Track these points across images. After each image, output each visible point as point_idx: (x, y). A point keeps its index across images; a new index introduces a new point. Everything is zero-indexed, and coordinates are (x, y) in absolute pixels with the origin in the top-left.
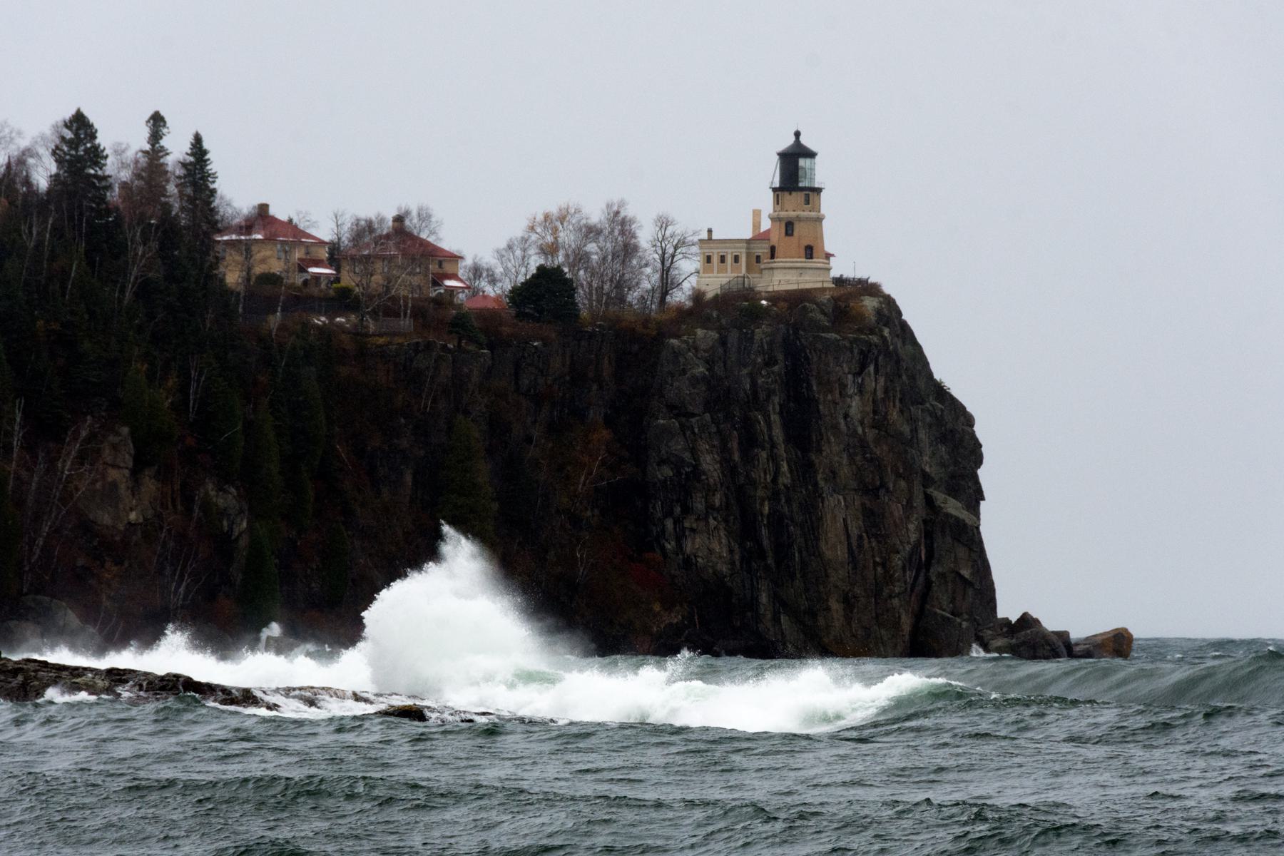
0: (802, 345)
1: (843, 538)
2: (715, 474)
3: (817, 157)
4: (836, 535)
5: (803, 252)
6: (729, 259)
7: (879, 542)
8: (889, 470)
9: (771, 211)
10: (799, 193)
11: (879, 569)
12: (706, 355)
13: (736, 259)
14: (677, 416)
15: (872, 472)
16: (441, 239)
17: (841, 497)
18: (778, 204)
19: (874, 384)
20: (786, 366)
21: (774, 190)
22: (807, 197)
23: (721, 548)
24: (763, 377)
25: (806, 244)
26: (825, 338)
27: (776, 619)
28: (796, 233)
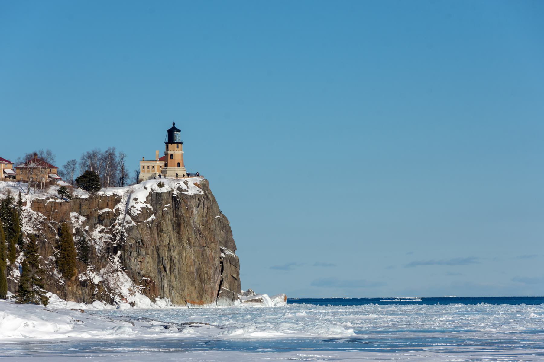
3: (181, 132)
5: (176, 165)
6: (151, 167)
7: (206, 265)
8: (208, 240)
11: (206, 275)
16: (55, 162)
17: (192, 250)
19: (203, 210)
21: (166, 143)
25: (178, 162)
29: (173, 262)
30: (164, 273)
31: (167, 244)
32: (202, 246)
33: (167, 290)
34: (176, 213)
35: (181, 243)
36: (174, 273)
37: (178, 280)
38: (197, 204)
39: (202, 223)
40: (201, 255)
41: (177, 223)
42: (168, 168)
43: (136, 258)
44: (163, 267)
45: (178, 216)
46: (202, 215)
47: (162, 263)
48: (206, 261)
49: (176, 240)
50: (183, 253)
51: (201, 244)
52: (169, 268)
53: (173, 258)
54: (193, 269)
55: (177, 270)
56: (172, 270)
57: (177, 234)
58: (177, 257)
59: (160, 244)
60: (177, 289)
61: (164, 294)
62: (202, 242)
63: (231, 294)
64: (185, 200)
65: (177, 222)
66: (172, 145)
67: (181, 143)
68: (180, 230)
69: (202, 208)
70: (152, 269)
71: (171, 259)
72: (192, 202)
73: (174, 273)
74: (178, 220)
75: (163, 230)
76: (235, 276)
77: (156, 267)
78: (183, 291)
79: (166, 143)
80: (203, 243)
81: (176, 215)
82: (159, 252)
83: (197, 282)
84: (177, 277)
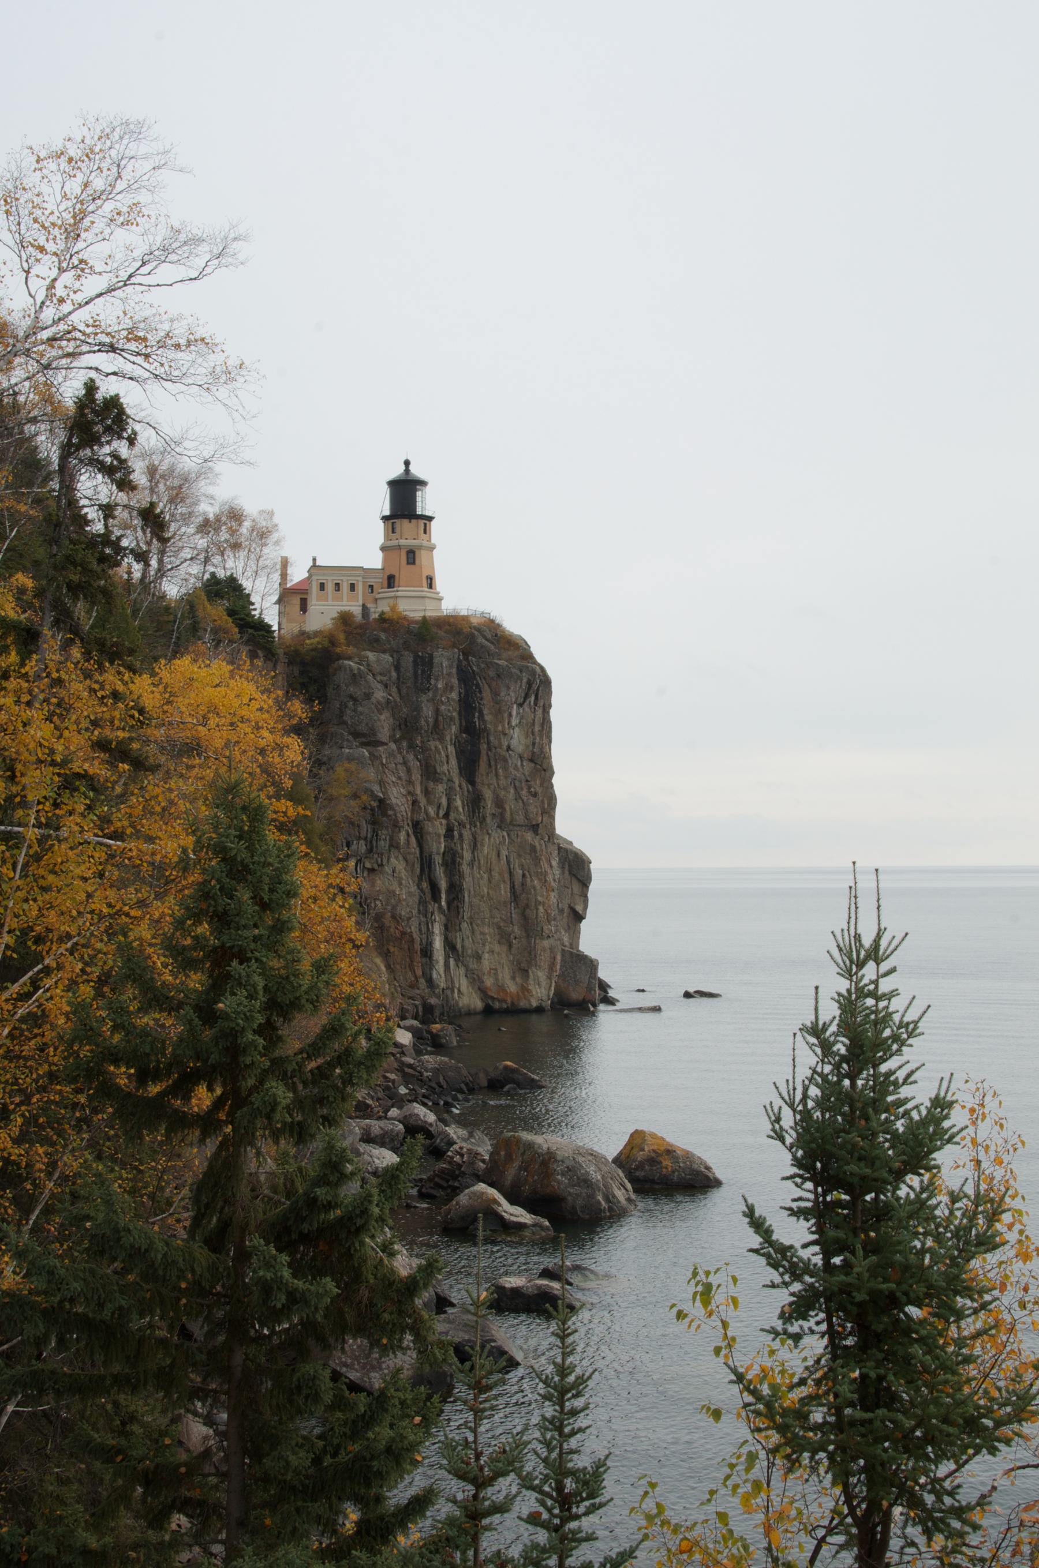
1: (507, 876)
2: (402, 808)
4: (500, 874)
5: (425, 582)
6: (345, 588)
9: (382, 540)
13: (352, 587)
14: (363, 745)
17: (505, 834)
20: (460, 693)
21: (385, 519)
22: (425, 524)
28: (417, 562)
30: (432, 906)
50: (482, 845)
64: (494, 684)
67: (430, 519)
70: (404, 892)
76: (579, 908)
77: (414, 889)
78: (478, 957)
79: (385, 519)
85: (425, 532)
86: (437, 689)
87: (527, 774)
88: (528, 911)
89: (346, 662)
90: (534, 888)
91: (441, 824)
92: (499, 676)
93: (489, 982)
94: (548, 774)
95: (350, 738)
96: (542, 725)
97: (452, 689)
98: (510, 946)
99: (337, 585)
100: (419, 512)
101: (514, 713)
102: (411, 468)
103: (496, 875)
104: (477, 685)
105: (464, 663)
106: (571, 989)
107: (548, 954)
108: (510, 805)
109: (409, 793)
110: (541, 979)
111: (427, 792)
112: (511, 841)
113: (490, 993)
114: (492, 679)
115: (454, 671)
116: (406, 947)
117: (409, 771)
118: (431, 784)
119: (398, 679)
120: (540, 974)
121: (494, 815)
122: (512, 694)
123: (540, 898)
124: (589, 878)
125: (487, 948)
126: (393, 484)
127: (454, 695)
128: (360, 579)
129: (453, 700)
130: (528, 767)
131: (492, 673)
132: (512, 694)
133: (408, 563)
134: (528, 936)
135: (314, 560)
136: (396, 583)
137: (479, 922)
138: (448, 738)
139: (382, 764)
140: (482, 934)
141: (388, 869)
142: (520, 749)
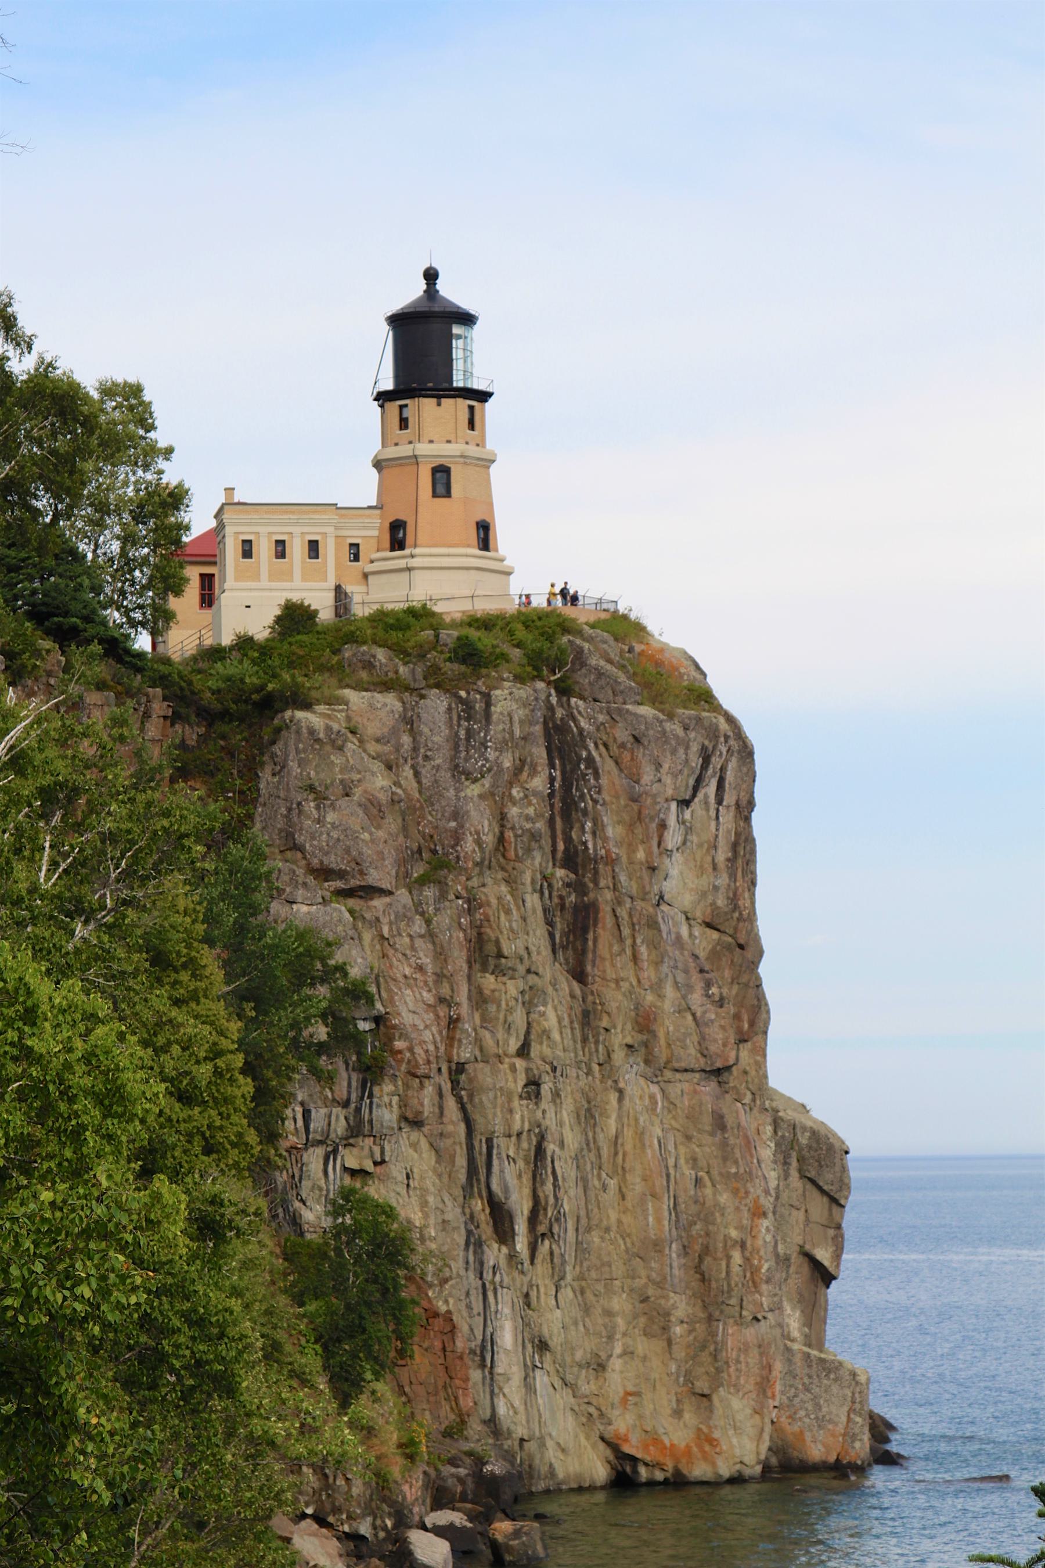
0: (581, 731)
2: (427, 1036)
4: (645, 1179)
6: (297, 550)
7: (735, 1192)
10: (460, 401)
11: (737, 1257)
12: (387, 748)
13: (314, 548)
15: (723, 1028)
18: (404, 423)
19: (713, 824)
20: (552, 780)
21: (382, 398)
22: (471, 408)
23: (426, 1216)
24: (514, 804)
25: (479, 518)
26: (635, 715)
27: (529, 1386)
29: (549, 1170)
31: (514, 1045)
32: (719, 1064)
33: (515, 1369)
34: (568, 840)
35: (597, 1042)
36: (552, 1253)
37: (571, 1294)
38: (692, 782)
39: (709, 910)
40: (707, 1122)
41: (577, 909)
42: (417, 551)
43: (335, 1152)
44: (488, 1211)
45: (579, 860)
46: (709, 859)
47: (483, 1178)
48: (736, 1162)
49: (566, 1022)
50: (605, 1114)
51: (713, 1048)
52: (526, 1212)
53: (551, 1147)
54: (659, 1220)
55: (570, 1225)
56: (542, 1229)
57: (575, 984)
58: (572, 1139)
59: (481, 1049)
60: (568, 1360)
61: (492, 1393)
62: (720, 1036)
63: (836, 1380)
64: (626, 756)
65: (573, 898)
66: (439, 404)
67: (483, 396)
68: (590, 955)
69: (713, 813)
70: (432, 1221)
71: (540, 1151)
72: (666, 766)
73: (552, 1253)
74: (579, 887)
75: (506, 951)
76: (823, 1255)
77: (453, 1213)
78: (601, 1367)
79: (382, 398)
80: (725, 1045)
81: (566, 850)
82: (468, 1106)
83: (681, 1306)
84: (569, 1277)
85: (471, 425)
86: (501, 770)
87: (702, 955)
88: (708, 1260)
89: (300, 714)
90: (722, 1211)
91: (513, 1069)
92: (637, 740)
93: (622, 1423)
94: (749, 954)
95: (310, 880)
96: (735, 847)
97: (534, 772)
98: (669, 1342)
99: (281, 543)
100: (458, 382)
101: (672, 821)
102: (441, 285)
103: (636, 1185)
104: (590, 761)
105: (560, 713)
106: (808, 1437)
107: (753, 1358)
108: (668, 1026)
109: (442, 1000)
110: (739, 1417)
111: (480, 999)
112: (671, 1105)
113: (627, 1449)
114: (622, 746)
115: (538, 729)
116: (438, 1344)
117: (441, 955)
118: (489, 981)
119: (415, 749)
120: (736, 1403)
121: (629, 1047)
122: (668, 780)
123: (734, 1234)
124: (844, 1184)
125: (618, 1350)
126: (399, 321)
127: (539, 783)
128: (330, 530)
129: (536, 793)
130: (704, 941)
131: (622, 734)
132: (668, 780)
133: (435, 495)
134: (710, 1318)
135: (230, 490)
136: (409, 540)
137: (600, 1287)
138: (527, 878)
139: (382, 937)
140: (609, 1313)
141: (397, 1171)
142: (687, 900)
